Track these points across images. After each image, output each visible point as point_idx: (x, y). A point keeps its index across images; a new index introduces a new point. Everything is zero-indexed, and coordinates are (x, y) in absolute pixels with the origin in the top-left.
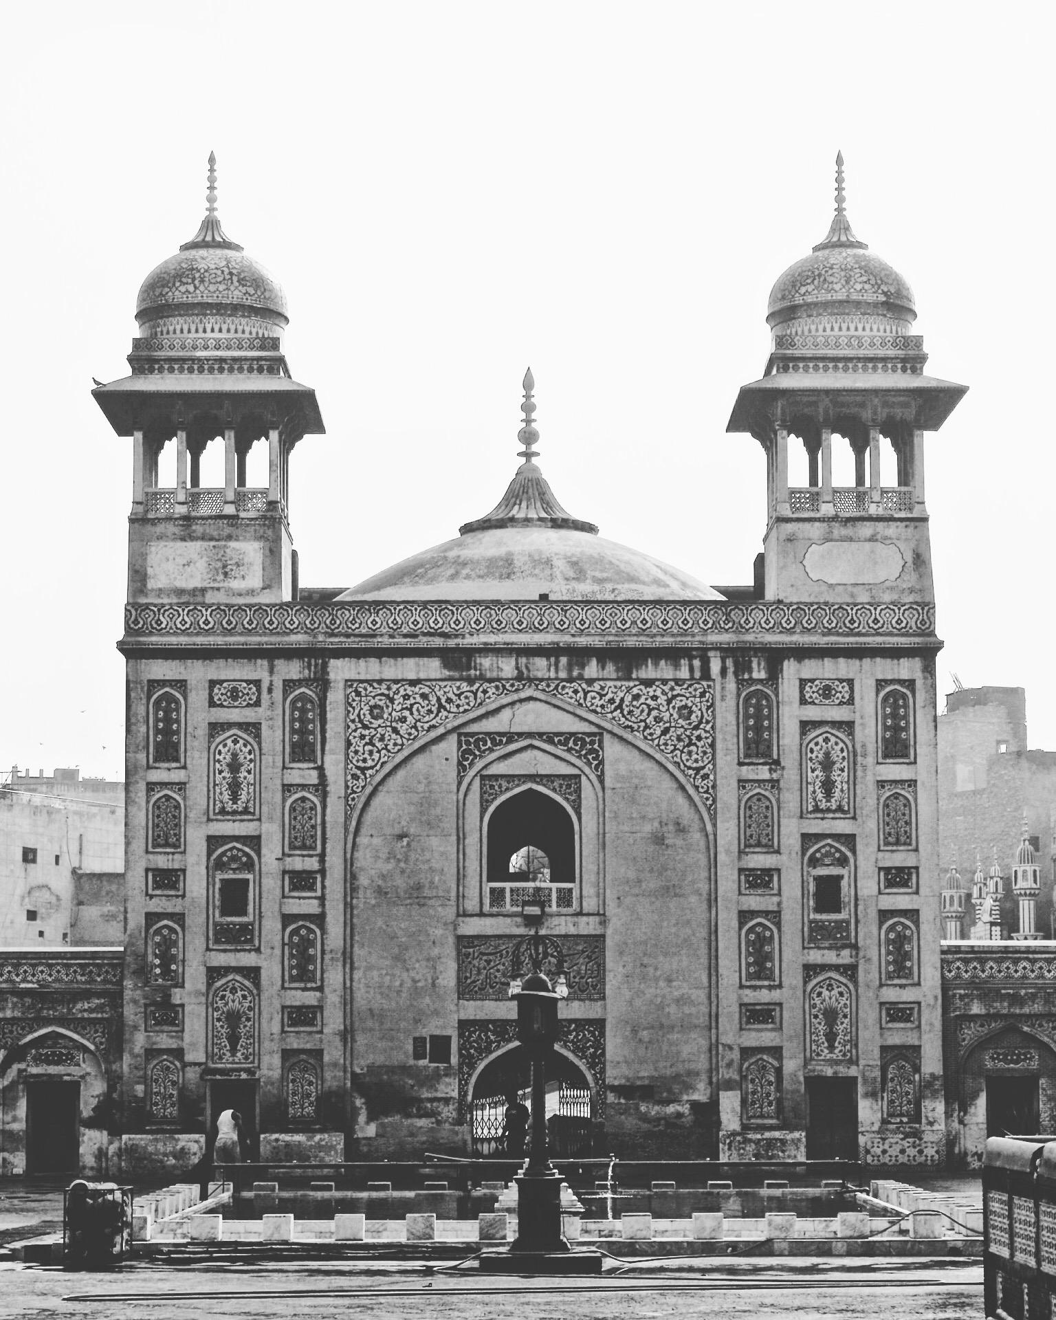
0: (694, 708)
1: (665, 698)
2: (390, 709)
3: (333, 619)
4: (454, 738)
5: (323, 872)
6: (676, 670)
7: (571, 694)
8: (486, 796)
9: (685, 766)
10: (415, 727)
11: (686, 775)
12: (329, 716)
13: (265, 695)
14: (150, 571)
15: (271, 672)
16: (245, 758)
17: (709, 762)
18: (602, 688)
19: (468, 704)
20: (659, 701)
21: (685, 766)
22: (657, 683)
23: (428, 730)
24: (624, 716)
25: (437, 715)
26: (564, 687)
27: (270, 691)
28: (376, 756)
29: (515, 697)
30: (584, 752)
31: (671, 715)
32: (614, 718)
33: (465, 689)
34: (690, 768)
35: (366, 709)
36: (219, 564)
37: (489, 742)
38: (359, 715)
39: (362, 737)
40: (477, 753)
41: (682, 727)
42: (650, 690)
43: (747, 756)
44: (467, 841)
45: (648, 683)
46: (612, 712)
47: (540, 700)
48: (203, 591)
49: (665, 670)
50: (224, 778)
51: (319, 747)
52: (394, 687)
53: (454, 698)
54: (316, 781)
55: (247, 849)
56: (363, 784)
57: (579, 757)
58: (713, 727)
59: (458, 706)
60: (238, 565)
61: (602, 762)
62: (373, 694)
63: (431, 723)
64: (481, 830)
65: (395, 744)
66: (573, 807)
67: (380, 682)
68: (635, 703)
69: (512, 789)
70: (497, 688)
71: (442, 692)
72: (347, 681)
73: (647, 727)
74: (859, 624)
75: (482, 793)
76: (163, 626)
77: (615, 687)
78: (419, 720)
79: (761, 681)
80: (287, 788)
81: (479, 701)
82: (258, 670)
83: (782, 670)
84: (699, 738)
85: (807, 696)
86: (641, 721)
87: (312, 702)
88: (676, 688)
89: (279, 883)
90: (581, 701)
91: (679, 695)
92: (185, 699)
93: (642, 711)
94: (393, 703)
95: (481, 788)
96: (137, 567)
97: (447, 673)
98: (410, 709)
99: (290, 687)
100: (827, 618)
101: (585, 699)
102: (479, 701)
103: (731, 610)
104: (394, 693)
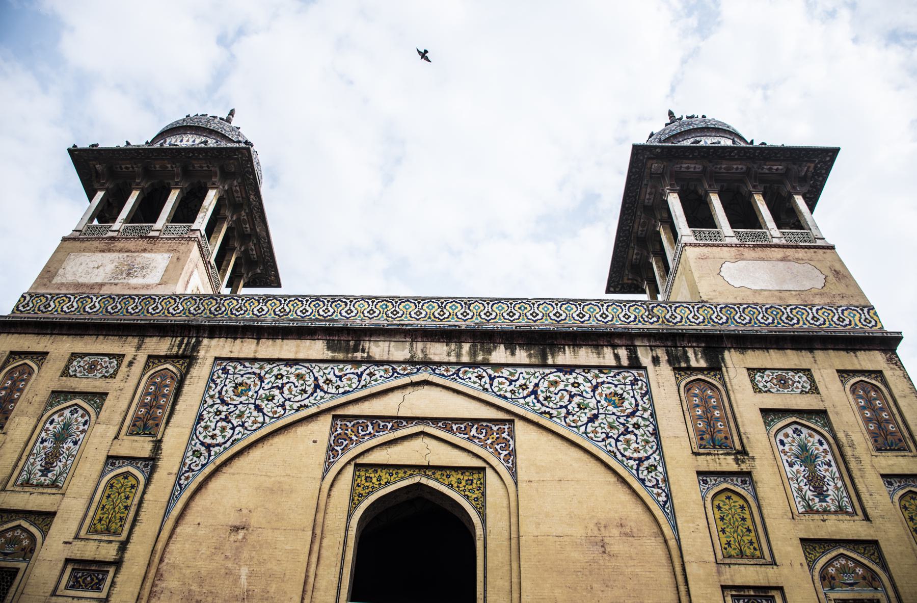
0: (625, 395)
1: (589, 385)
2: (258, 387)
3: (219, 307)
4: (327, 420)
5: (118, 564)
6: (599, 357)
7: (474, 379)
8: (359, 490)
9: (623, 455)
10: (283, 406)
11: (626, 467)
12: (186, 389)
13: (124, 368)
14: (61, 271)
15: (139, 348)
16: (78, 428)
17: (654, 452)
18: (512, 374)
19: (350, 386)
20: (582, 387)
21: (623, 455)
22: (577, 371)
23: (297, 410)
24: (539, 401)
25: (312, 394)
26: (465, 372)
27: (131, 364)
28: (229, 433)
29: (406, 380)
30: (489, 442)
31: (599, 402)
32: (527, 404)
33: (348, 371)
34: (631, 458)
35: (229, 387)
36: (126, 267)
37: (370, 428)
38: (220, 393)
39: (218, 413)
40: (354, 438)
41: (613, 414)
42: (570, 377)
43: (700, 447)
44: (325, 542)
45: (568, 369)
46: (524, 398)
47: (437, 385)
48: (102, 285)
49: (585, 356)
50: (44, 448)
51: (164, 421)
52: (267, 367)
53: (334, 379)
54: (146, 453)
55: (33, 529)
56: (205, 462)
57: (484, 446)
58: (651, 415)
59: (338, 387)
60: (143, 268)
61: (513, 453)
62: (242, 373)
63: (302, 403)
64: (347, 530)
65: (255, 422)
66: (475, 508)
67: (254, 360)
68: (552, 389)
69: (395, 483)
70: (386, 371)
71: (321, 373)
72: (216, 359)
73: (568, 413)
74: (798, 320)
75: (355, 485)
76: (50, 309)
77: (528, 373)
78: (289, 400)
79: (700, 370)
80: (112, 460)
81: (363, 383)
82: (127, 347)
83: (723, 359)
84: (637, 426)
85: (760, 385)
86: (561, 407)
87: (172, 378)
88: (601, 375)
89: (57, 572)
90: (487, 386)
91: (603, 383)
92: (39, 368)
93: (562, 398)
94: (262, 381)
95: (354, 480)
96: (52, 269)
97: (329, 355)
98: (281, 389)
99: (154, 363)
100: (761, 315)
101: (491, 385)
102: (363, 383)
103: (653, 307)
104: (266, 373)
